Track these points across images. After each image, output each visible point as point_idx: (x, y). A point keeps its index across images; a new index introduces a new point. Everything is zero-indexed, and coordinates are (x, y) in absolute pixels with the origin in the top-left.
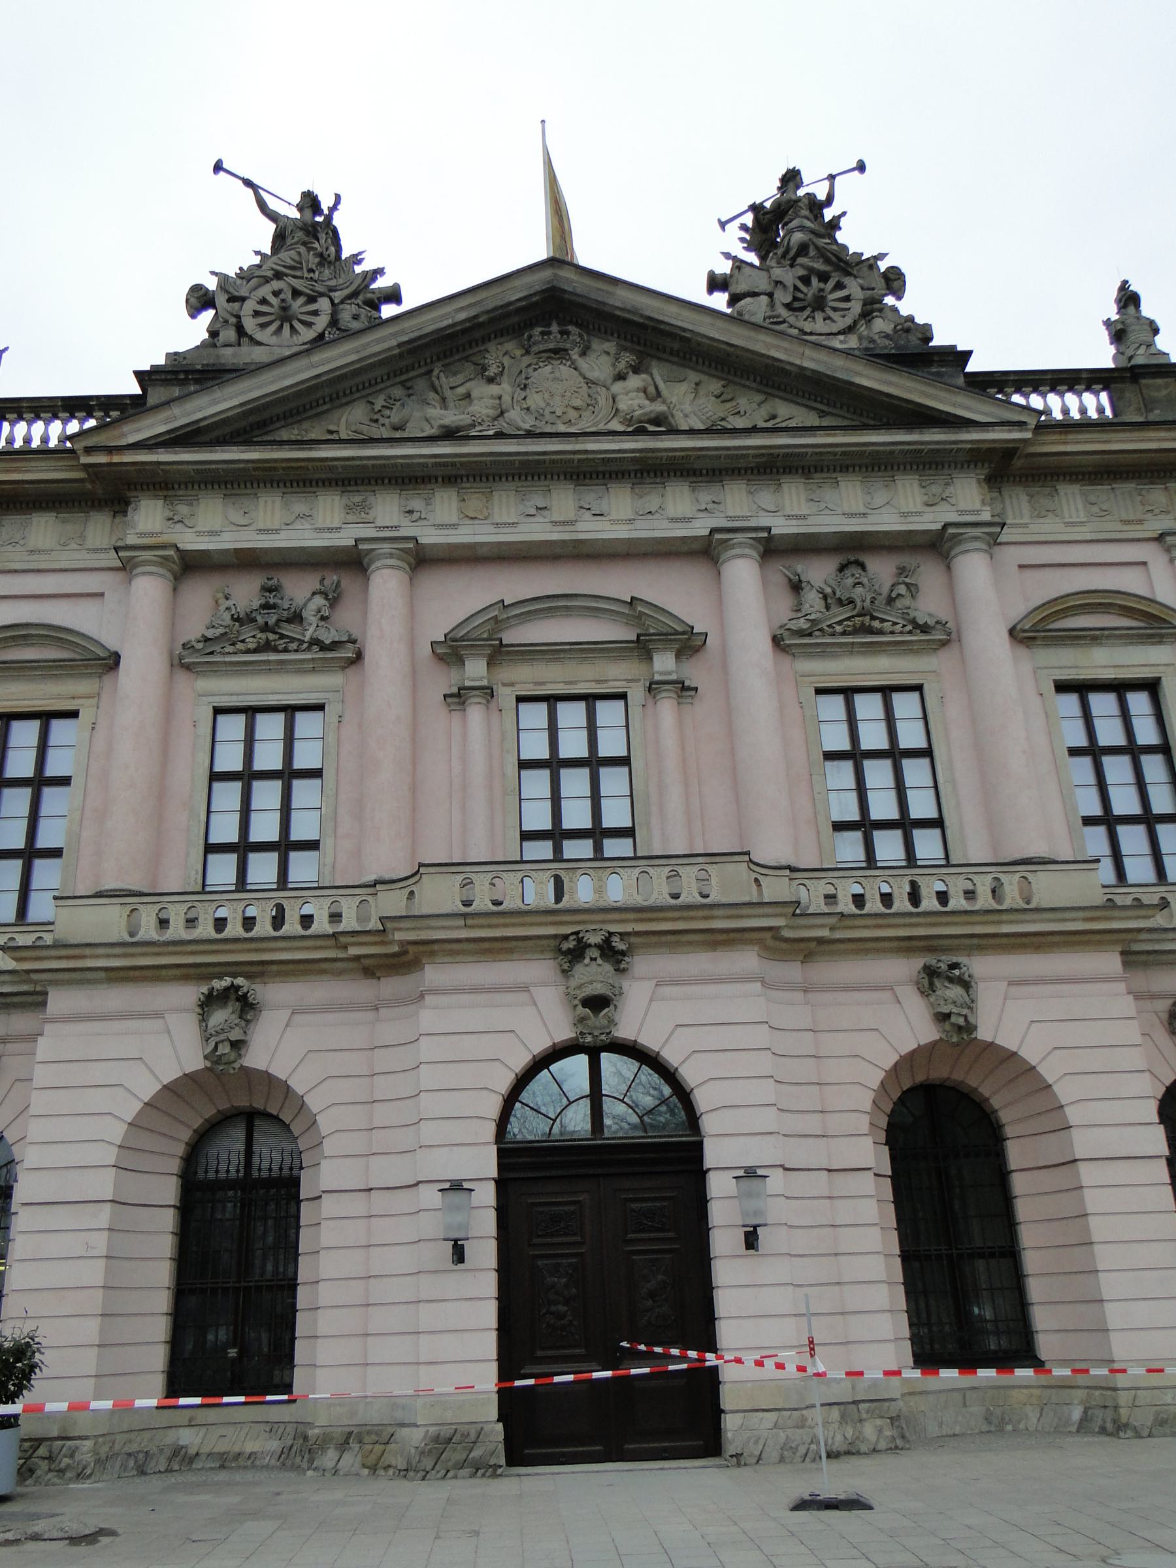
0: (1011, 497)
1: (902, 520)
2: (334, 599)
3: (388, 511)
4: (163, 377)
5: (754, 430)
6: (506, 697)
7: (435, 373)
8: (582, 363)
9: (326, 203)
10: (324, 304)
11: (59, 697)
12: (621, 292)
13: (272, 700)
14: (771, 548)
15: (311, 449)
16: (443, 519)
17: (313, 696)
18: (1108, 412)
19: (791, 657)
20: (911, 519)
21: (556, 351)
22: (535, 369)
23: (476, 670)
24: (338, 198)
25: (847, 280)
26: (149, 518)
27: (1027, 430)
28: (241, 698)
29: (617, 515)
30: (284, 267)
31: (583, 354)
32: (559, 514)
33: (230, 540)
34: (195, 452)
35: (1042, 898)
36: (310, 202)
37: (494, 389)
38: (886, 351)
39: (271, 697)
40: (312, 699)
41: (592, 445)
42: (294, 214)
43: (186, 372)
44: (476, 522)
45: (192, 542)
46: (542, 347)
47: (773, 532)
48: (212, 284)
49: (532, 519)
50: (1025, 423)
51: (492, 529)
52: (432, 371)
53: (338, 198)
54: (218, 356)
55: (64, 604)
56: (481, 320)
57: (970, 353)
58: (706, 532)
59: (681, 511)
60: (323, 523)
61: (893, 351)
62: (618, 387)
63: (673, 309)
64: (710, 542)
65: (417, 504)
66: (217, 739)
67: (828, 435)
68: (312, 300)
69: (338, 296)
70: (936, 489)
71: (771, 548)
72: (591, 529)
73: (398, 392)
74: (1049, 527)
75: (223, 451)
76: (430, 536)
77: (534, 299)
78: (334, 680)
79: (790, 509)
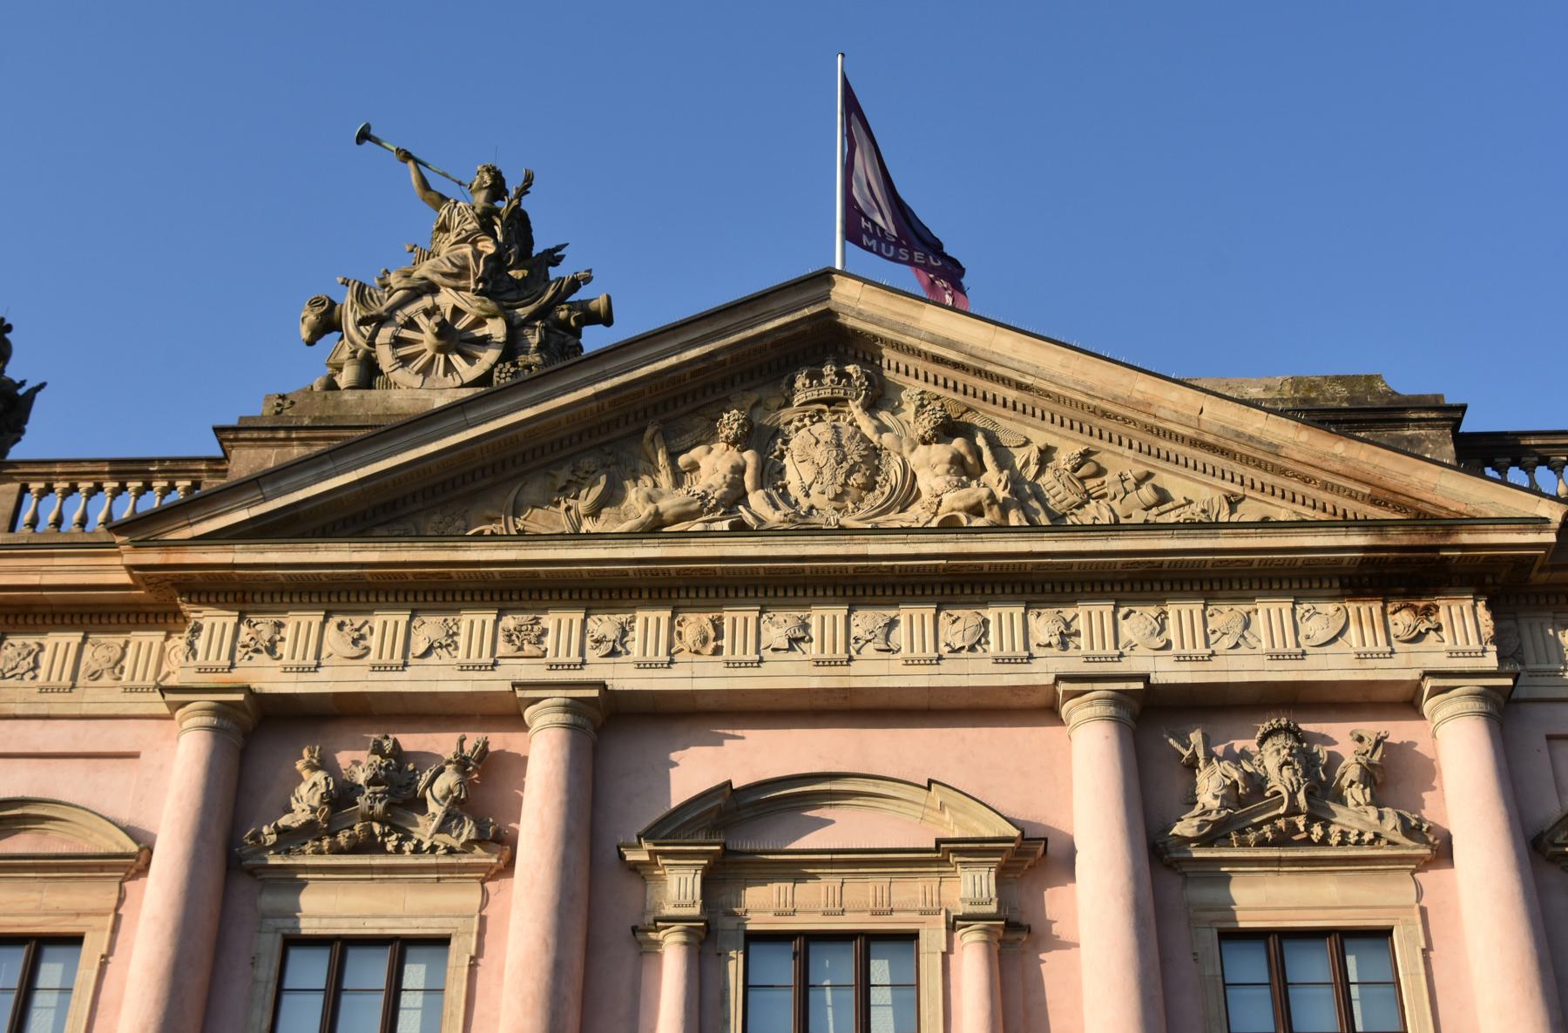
0: (1530, 626)
1: (1357, 664)
4: (255, 435)
5: (1116, 527)
7: (649, 433)
9: (512, 187)
11: (58, 912)
13: (371, 928)
15: (455, 548)
17: (435, 922)
19: (1180, 879)
20: (1370, 663)
21: (829, 402)
22: (798, 429)
24: (529, 180)
27: (1547, 530)
28: (325, 922)
29: (910, 647)
30: (444, 275)
34: (285, 550)
38: (1334, 404)
39: (369, 923)
40: (431, 928)
43: (289, 429)
44: (697, 658)
46: (813, 395)
47: (1152, 681)
49: (781, 655)
50: (1546, 520)
51: (720, 669)
52: (645, 429)
53: (529, 180)
54: (337, 405)
56: (721, 358)
57: (1463, 408)
58: (1050, 680)
61: (1345, 405)
64: (1056, 693)
66: (288, 984)
67: (1236, 536)
72: (874, 672)
75: (327, 550)
77: (801, 328)
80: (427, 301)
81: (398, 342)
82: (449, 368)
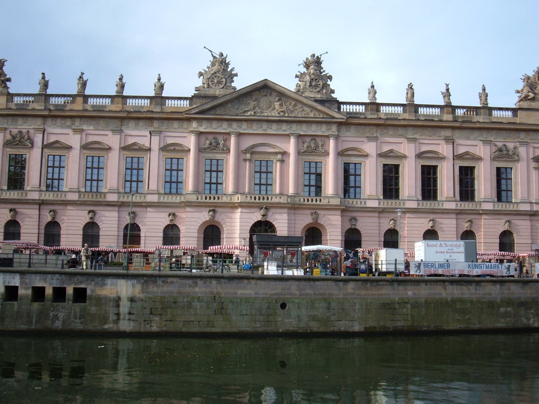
2: (225, 140)
3: (235, 127)
6: (253, 160)
8: (270, 98)
9: (225, 56)
10: (224, 80)
12: (278, 86)
14: (299, 136)
16: (244, 128)
18: (364, 111)
23: (248, 156)
25: (320, 81)
26: (194, 124)
29: (273, 129)
31: (270, 96)
32: (263, 129)
33: (208, 130)
35: (331, 203)
36: (222, 55)
37: (254, 103)
40: (222, 158)
41: (270, 118)
42: (218, 57)
45: (202, 129)
48: (203, 71)
55: (179, 139)
59: (285, 129)
60: (224, 128)
62: (276, 103)
63: (286, 91)
65: (240, 125)
68: (222, 78)
69: (226, 77)
70: (329, 127)
71: (299, 136)
72: (269, 132)
73: (237, 102)
74: (348, 134)
76: (242, 131)
78: (225, 155)
79: (303, 130)
80: (215, 75)
81: (212, 81)
82: (218, 86)
